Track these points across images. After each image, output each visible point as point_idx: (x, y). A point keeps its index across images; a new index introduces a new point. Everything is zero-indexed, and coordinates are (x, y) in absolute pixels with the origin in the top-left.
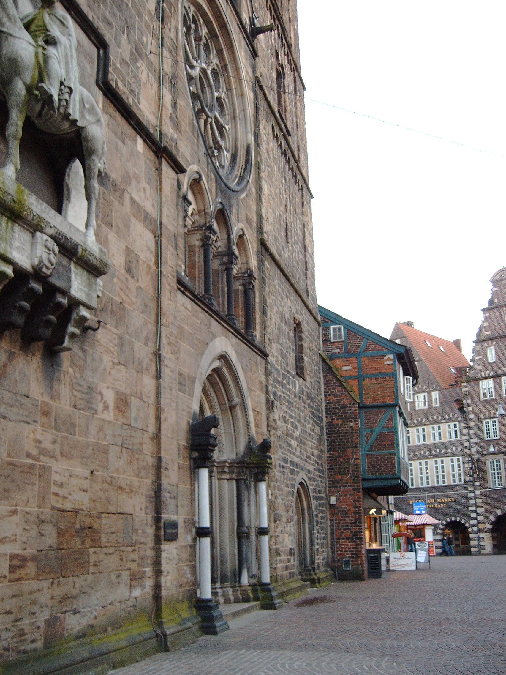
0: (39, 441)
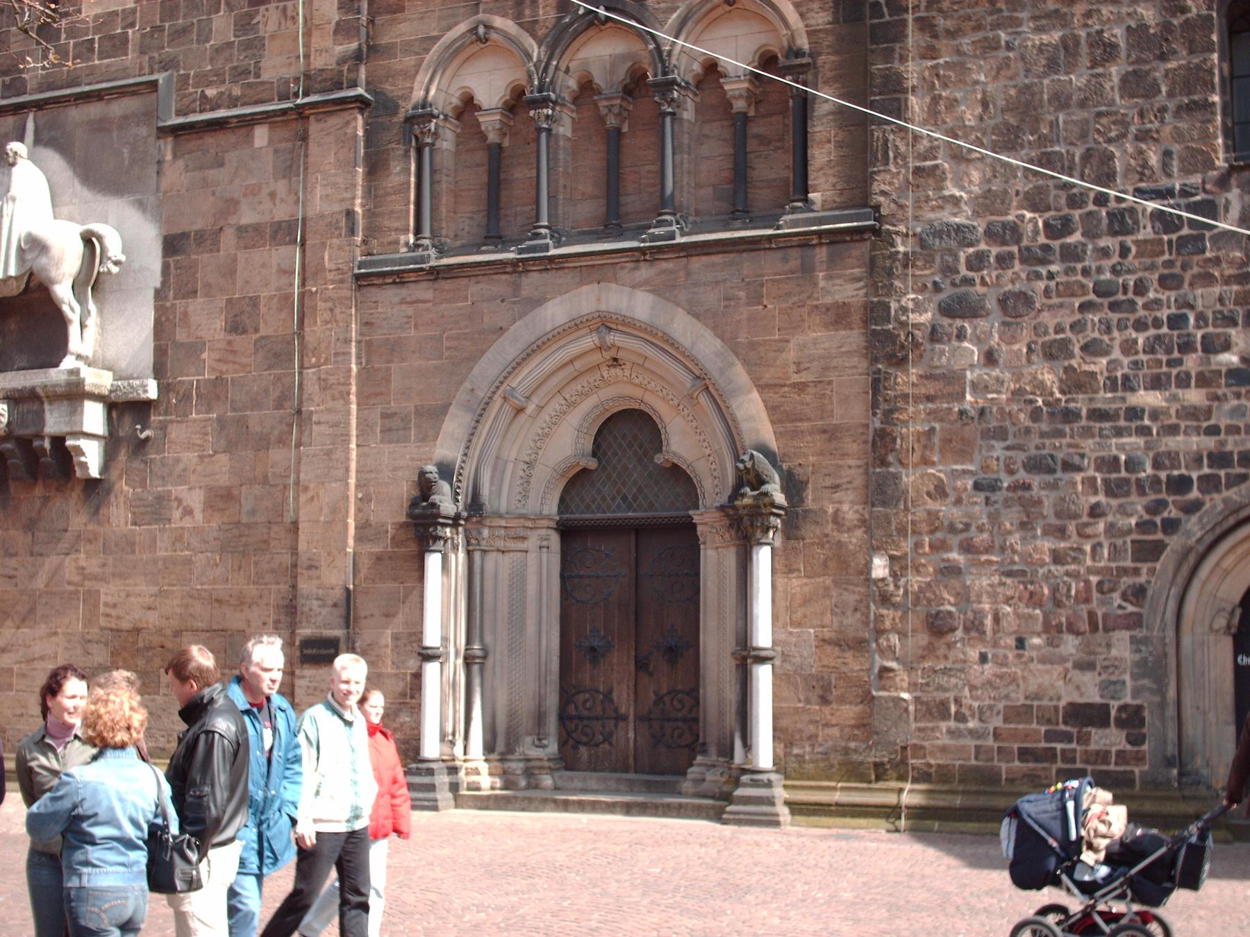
0: (83, 568)
